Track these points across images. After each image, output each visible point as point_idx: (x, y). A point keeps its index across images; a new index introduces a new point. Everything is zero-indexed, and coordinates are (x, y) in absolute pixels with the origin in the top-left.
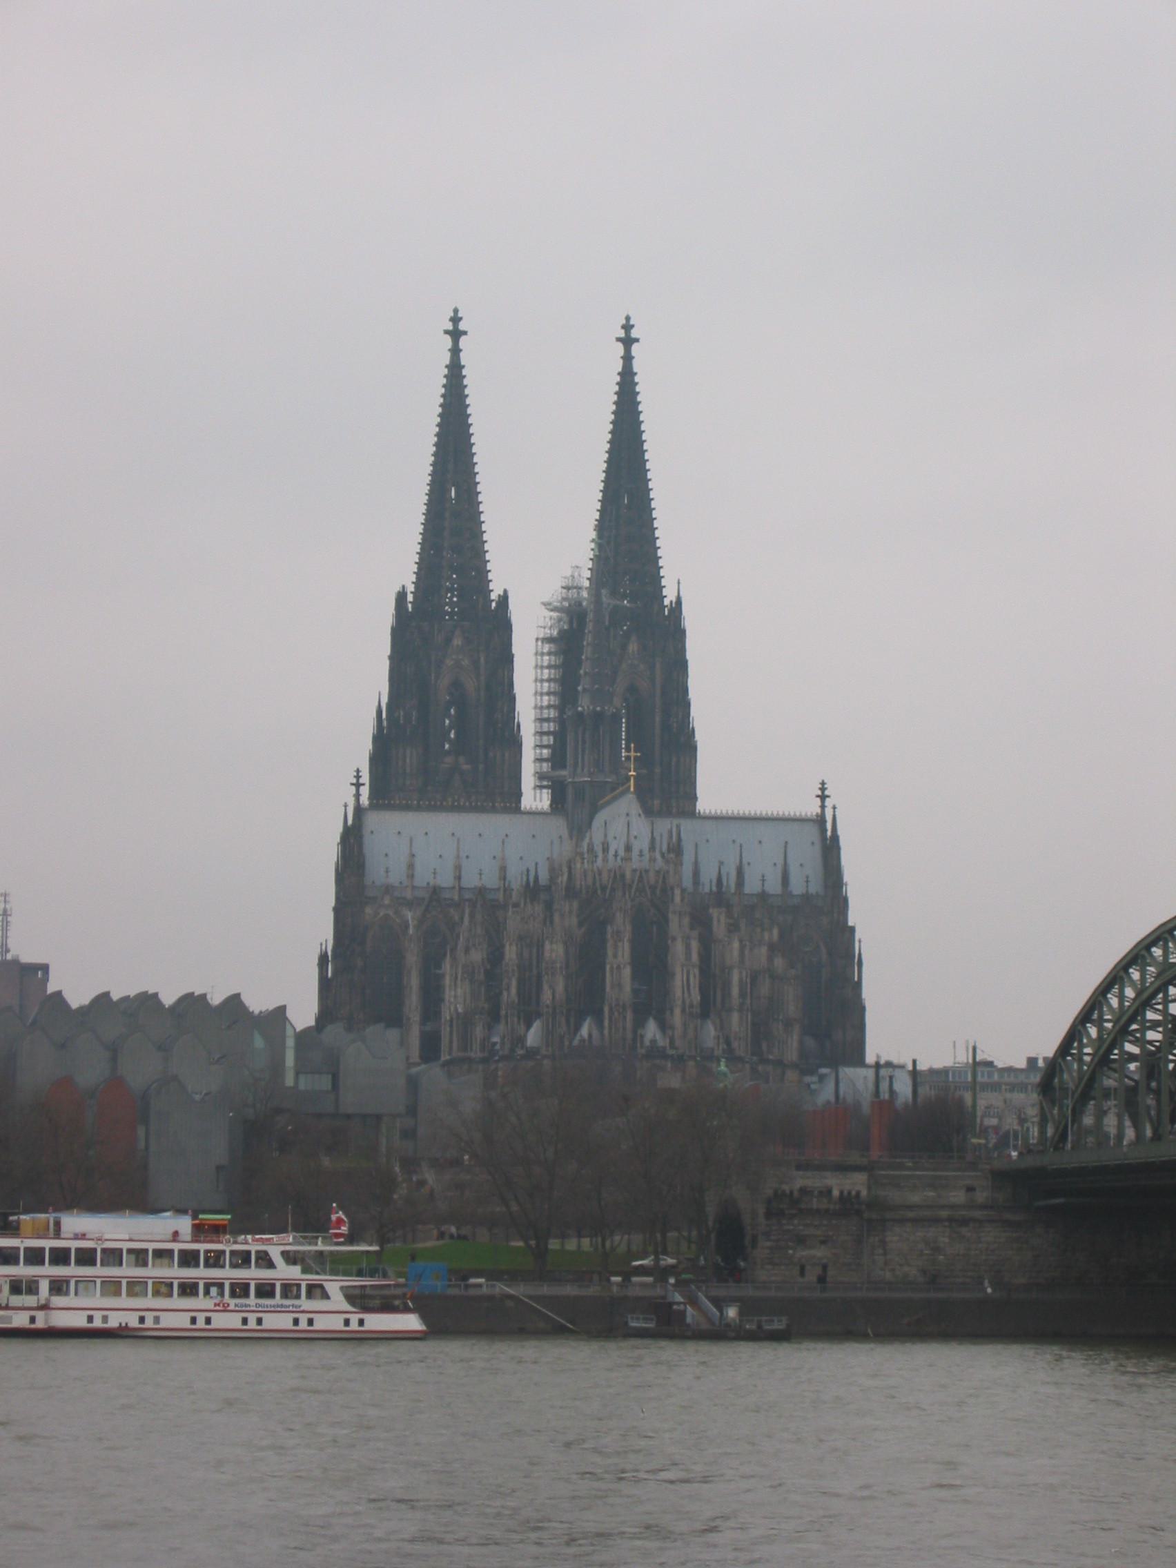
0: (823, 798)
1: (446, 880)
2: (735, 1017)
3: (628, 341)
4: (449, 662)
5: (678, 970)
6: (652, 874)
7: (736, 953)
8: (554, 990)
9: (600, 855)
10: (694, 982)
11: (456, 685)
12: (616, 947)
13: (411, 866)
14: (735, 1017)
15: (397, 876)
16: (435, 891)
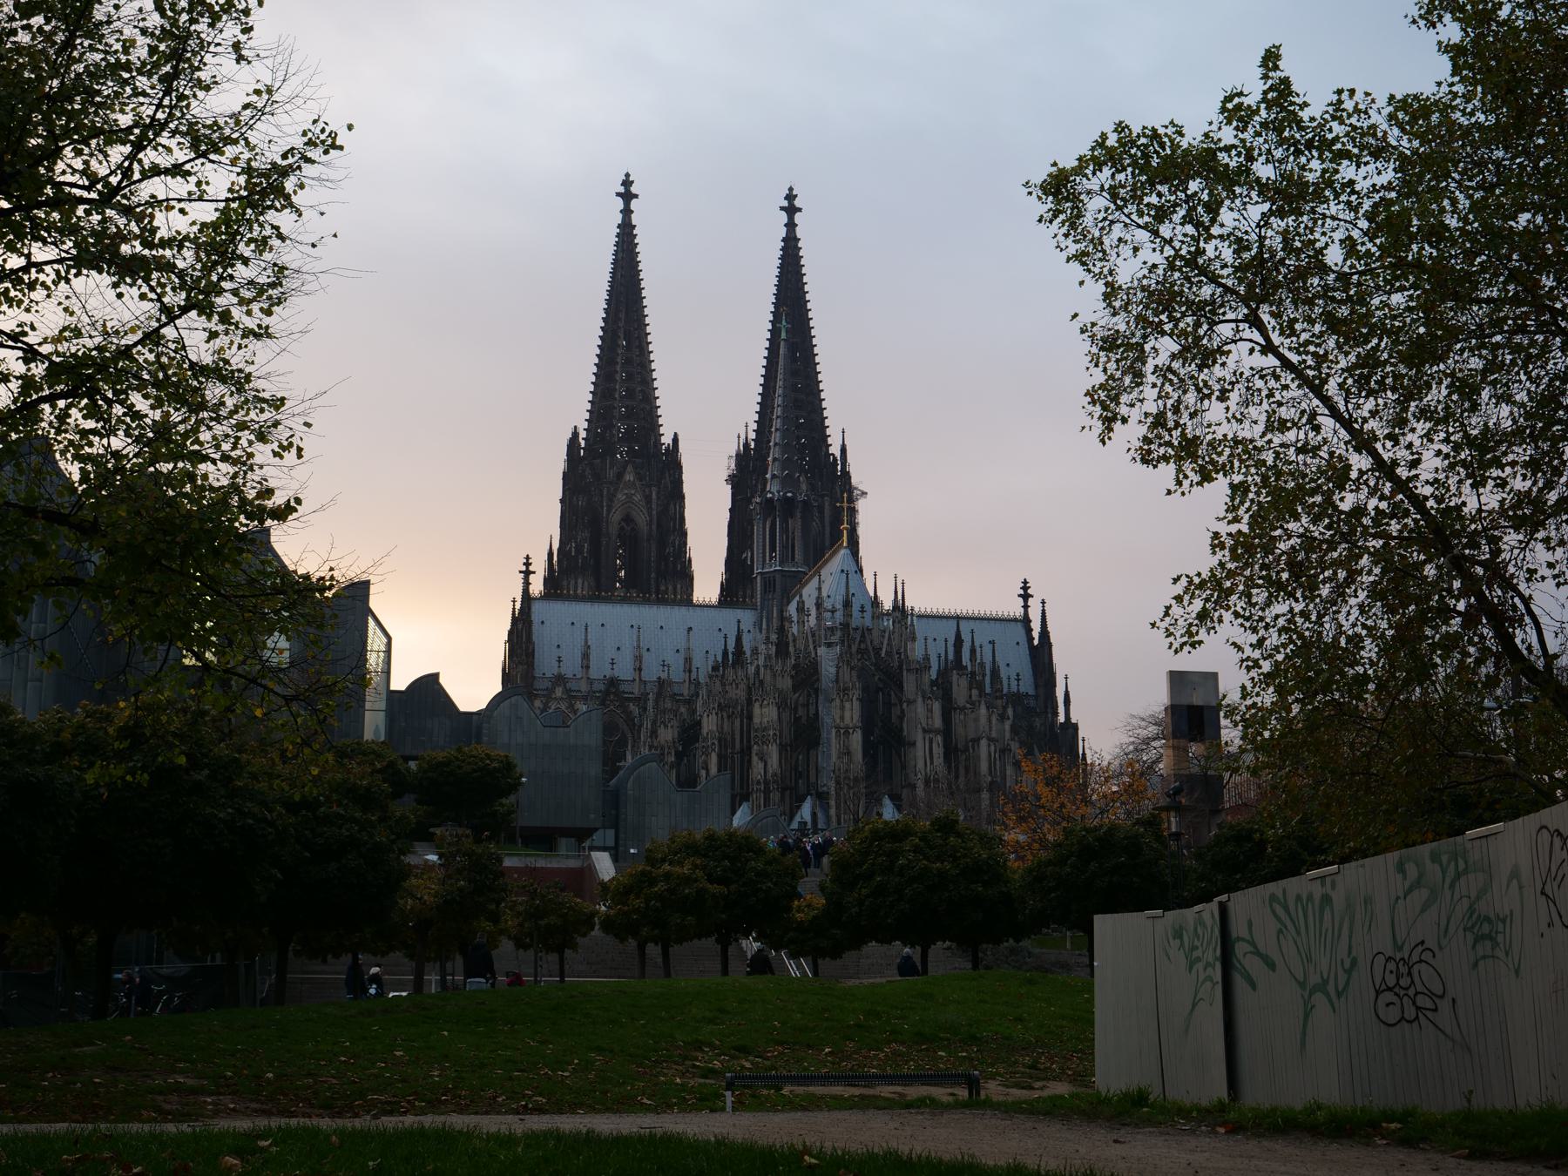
0: (1026, 596)
1: (625, 671)
2: (985, 795)
3: (791, 210)
4: (621, 496)
5: (919, 738)
6: (875, 633)
7: (983, 721)
8: (768, 762)
9: (813, 612)
10: (938, 751)
11: (628, 519)
12: (842, 708)
13: (586, 656)
14: (985, 795)
15: (571, 667)
16: (613, 682)
